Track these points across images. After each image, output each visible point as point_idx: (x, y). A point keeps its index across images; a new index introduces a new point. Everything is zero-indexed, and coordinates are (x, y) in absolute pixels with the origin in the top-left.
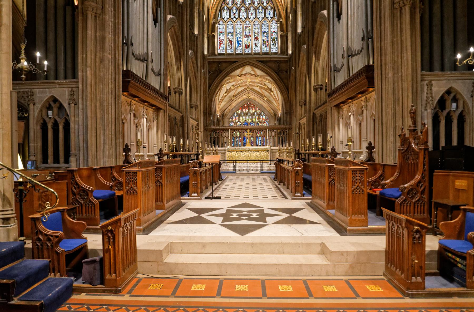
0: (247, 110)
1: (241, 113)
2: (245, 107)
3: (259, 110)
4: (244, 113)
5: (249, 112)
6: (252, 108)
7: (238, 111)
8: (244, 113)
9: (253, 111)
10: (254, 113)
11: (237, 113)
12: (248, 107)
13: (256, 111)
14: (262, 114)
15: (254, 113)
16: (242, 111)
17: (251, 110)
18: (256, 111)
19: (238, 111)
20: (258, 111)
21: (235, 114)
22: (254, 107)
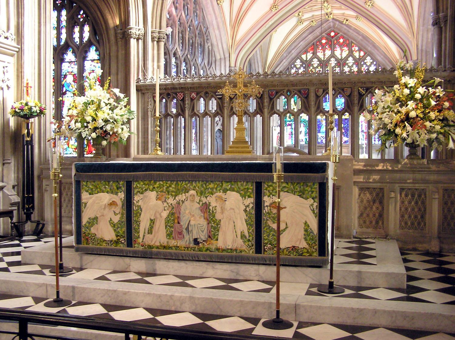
0: (328, 53)
1: (312, 59)
2: (323, 46)
3: (360, 50)
4: (319, 60)
5: (333, 56)
6: (341, 46)
7: (304, 57)
8: (319, 60)
9: (345, 54)
10: (347, 58)
11: (302, 61)
12: (332, 43)
13: (351, 54)
14: (368, 60)
15: (347, 58)
16: (315, 55)
17: (338, 53)
18: (351, 54)
19: (304, 57)
20: (357, 55)
21: (298, 63)
22: (349, 44)
